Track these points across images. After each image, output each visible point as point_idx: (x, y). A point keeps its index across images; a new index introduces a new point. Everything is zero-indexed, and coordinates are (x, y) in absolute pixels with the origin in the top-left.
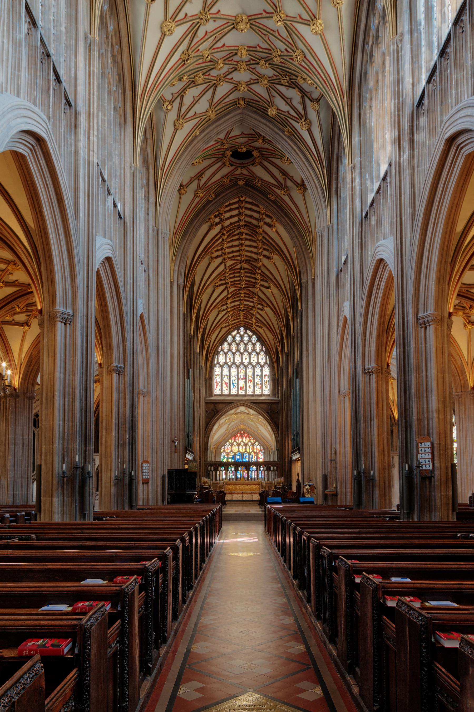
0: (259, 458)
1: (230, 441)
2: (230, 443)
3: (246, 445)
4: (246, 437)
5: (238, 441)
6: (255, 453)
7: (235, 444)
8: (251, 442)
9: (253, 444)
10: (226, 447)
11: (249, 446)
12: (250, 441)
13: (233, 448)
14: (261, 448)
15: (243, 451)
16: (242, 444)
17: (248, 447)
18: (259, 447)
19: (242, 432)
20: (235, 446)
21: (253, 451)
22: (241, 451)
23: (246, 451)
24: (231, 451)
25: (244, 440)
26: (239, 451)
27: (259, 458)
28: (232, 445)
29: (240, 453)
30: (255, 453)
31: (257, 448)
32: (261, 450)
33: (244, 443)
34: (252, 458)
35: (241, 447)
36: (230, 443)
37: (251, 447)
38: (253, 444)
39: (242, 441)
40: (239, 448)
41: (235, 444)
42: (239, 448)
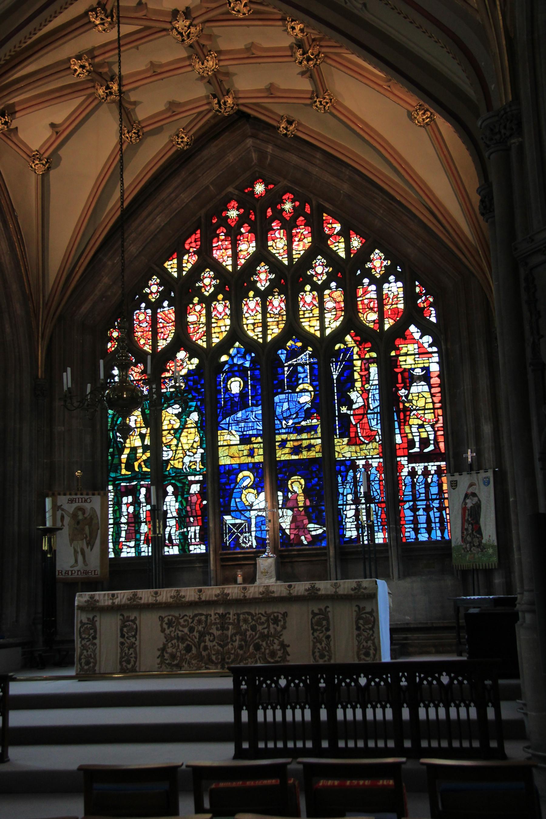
0: (409, 379)
1: (171, 266)
2: (166, 279)
3: (291, 280)
4: (289, 227)
5: (228, 263)
6: (365, 335)
7: (208, 282)
8: (331, 258)
9: (348, 274)
10: (142, 316)
11: (320, 289)
12: (320, 246)
13: (195, 316)
14: (410, 297)
15: (274, 331)
16: (263, 278)
17: (308, 297)
18: (394, 288)
19: (259, 188)
20: (208, 301)
21: (351, 322)
22: (254, 333)
23: (293, 327)
24: (182, 340)
25: (278, 245)
26: (236, 332)
27: (409, 379)
28: (181, 293)
29: (250, 345)
30: (365, 335)
31: (381, 298)
32: (412, 314)
33: (274, 265)
34: (347, 382)
35: (252, 304)
36: (166, 279)
37: (334, 297)
38: (348, 274)
39: (263, 255)
40: (237, 315)
41: (208, 282)
42: (237, 315)
